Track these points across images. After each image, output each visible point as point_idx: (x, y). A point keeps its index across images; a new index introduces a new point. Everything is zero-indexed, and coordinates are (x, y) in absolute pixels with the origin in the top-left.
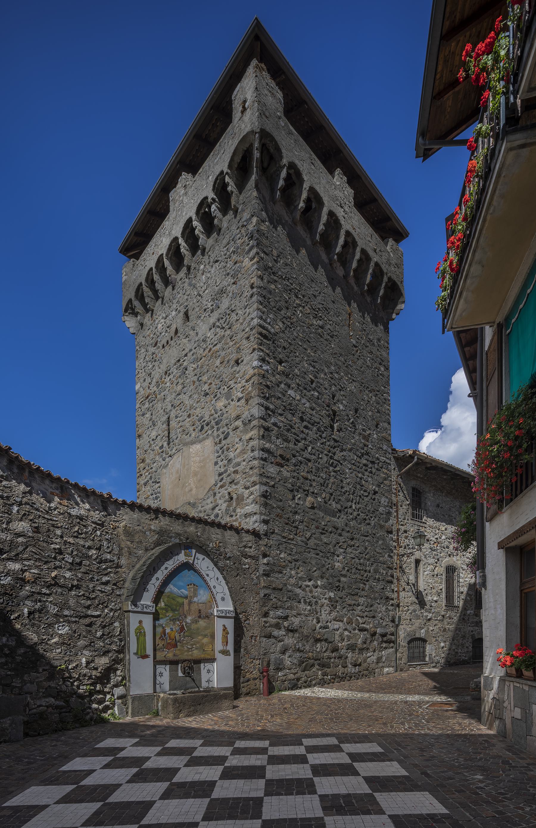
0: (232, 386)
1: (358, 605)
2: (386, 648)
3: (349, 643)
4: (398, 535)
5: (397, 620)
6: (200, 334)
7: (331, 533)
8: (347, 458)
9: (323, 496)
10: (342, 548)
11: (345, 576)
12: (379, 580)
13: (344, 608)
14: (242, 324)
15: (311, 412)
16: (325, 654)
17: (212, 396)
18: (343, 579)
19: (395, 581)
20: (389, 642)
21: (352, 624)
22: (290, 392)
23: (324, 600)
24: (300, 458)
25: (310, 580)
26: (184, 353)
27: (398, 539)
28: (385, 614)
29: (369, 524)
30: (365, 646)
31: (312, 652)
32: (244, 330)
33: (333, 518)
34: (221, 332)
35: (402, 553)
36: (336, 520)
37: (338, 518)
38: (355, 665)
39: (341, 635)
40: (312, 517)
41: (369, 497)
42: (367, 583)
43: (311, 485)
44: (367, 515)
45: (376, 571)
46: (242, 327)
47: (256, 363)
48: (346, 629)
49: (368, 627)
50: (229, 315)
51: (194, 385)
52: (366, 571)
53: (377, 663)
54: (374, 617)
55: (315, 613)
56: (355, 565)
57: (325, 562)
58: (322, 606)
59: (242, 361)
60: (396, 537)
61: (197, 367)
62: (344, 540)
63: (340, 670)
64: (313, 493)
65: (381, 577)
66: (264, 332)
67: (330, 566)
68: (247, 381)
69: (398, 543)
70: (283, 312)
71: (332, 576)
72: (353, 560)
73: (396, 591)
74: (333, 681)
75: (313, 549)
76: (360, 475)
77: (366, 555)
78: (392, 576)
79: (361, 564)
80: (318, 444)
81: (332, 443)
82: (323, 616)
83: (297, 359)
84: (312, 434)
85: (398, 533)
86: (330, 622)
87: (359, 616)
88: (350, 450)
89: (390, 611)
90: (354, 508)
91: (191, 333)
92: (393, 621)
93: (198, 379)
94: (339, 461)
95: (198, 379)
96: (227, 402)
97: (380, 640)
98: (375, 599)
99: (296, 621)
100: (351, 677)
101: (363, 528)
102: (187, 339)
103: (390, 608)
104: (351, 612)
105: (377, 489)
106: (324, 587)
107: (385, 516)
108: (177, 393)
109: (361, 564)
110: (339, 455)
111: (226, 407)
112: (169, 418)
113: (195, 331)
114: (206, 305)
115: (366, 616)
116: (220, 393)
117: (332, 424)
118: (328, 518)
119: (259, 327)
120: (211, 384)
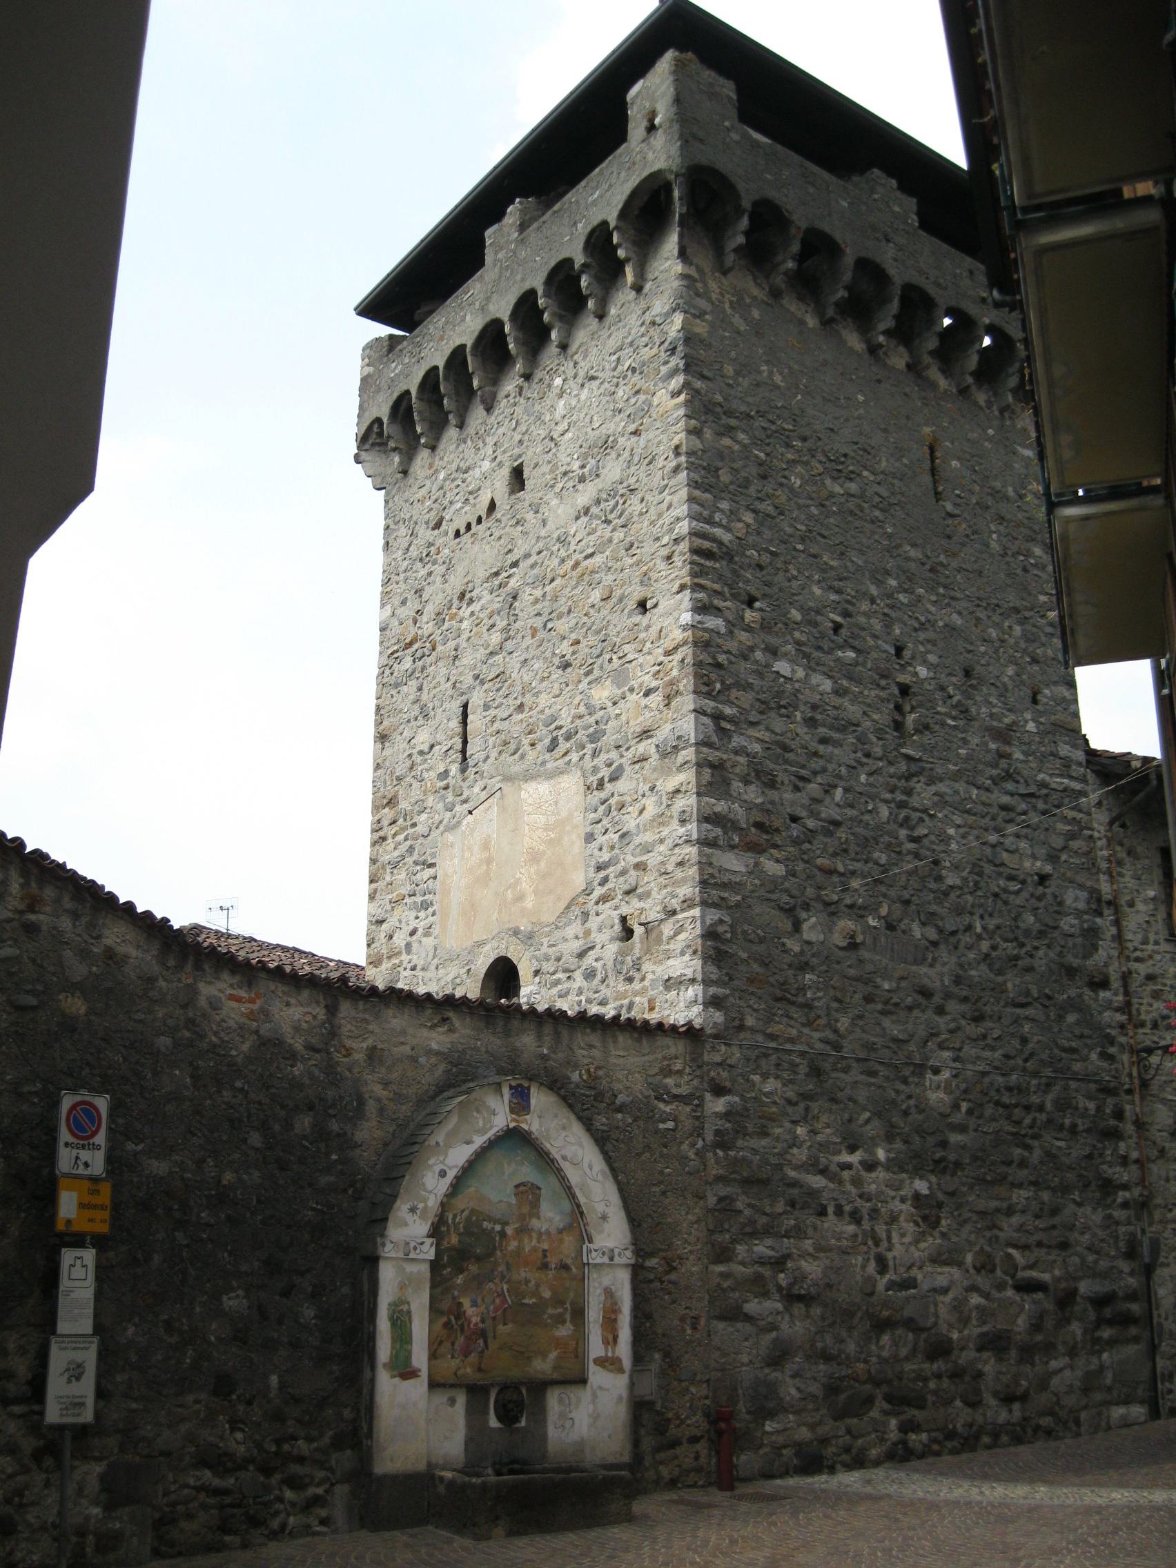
0: (630, 657)
1: (1010, 1212)
2: (1112, 1343)
3: (985, 1329)
4: (1126, 993)
6: (550, 525)
7: (910, 1009)
8: (947, 798)
9: (884, 911)
10: (948, 1049)
11: (962, 1129)
12: (1073, 1130)
13: (965, 1221)
14: (653, 523)
15: (837, 701)
16: (908, 1367)
17: (582, 672)
18: (955, 1138)
19: (1129, 1128)
20: (1126, 1320)
21: (993, 1271)
23: (897, 1202)
24: (811, 823)
26: (511, 558)
27: (1128, 1004)
28: (1101, 1234)
29: (1030, 969)
30: (1039, 1338)
31: (866, 1361)
32: (657, 539)
33: (914, 968)
34: (604, 531)
35: (1148, 1043)
36: (924, 970)
37: (931, 966)
39: (958, 1306)
41: (1025, 894)
42: (1036, 1143)
44: (1022, 945)
45: (1064, 1105)
46: (656, 531)
47: (687, 617)
48: (973, 1288)
49: (1046, 1277)
50: (622, 496)
51: (533, 637)
52: (1027, 1108)
53: (1086, 1390)
54: (1064, 1246)
55: (870, 1243)
56: (993, 1093)
57: (898, 1092)
58: (893, 1219)
59: (655, 606)
60: (1120, 998)
61: (544, 595)
62: (952, 1025)
63: (960, 1415)
64: (851, 907)
65: (1079, 1121)
66: (706, 544)
67: (912, 1102)
68: (668, 653)
69: (1130, 1014)
70: (752, 490)
71: (920, 1131)
72: (987, 1080)
73: (1137, 1161)
74: (936, 1447)
76: (993, 838)
77: (1026, 1060)
79: (1009, 1089)
80: (863, 778)
81: (903, 766)
82: (898, 1251)
83: (795, 584)
84: (843, 754)
85: (1125, 985)
86: (920, 1268)
87: (1015, 1246)
88: (956, 777)
89: (1117, 1223)
90: (979, 930)
91: (529, 515)
92: (1131, 1253)
93: (545, 625)
94: (925, 811)
95: (545, 625)
96: (619, 692)
97: (1092, 1316)
98: (1065, 1189)
100: (996, 1436)
101: (1012, 983)
102: (519, 528)
103: (1117, 1214)
104: (988, 1234)
105: (1048, 869)
106: (894, 1165)
107: (1079, 940)
108: (491, 649)
109: (1009, 1089)
110: (924, 794)
111: (615, 704)
113: (539, 515)
114: (568, 464)
115: (1040, 1244)
116: (601, 667)
117: (898, 718)
118: (901, 969)
119: (694, 539)
120: (577, 642)
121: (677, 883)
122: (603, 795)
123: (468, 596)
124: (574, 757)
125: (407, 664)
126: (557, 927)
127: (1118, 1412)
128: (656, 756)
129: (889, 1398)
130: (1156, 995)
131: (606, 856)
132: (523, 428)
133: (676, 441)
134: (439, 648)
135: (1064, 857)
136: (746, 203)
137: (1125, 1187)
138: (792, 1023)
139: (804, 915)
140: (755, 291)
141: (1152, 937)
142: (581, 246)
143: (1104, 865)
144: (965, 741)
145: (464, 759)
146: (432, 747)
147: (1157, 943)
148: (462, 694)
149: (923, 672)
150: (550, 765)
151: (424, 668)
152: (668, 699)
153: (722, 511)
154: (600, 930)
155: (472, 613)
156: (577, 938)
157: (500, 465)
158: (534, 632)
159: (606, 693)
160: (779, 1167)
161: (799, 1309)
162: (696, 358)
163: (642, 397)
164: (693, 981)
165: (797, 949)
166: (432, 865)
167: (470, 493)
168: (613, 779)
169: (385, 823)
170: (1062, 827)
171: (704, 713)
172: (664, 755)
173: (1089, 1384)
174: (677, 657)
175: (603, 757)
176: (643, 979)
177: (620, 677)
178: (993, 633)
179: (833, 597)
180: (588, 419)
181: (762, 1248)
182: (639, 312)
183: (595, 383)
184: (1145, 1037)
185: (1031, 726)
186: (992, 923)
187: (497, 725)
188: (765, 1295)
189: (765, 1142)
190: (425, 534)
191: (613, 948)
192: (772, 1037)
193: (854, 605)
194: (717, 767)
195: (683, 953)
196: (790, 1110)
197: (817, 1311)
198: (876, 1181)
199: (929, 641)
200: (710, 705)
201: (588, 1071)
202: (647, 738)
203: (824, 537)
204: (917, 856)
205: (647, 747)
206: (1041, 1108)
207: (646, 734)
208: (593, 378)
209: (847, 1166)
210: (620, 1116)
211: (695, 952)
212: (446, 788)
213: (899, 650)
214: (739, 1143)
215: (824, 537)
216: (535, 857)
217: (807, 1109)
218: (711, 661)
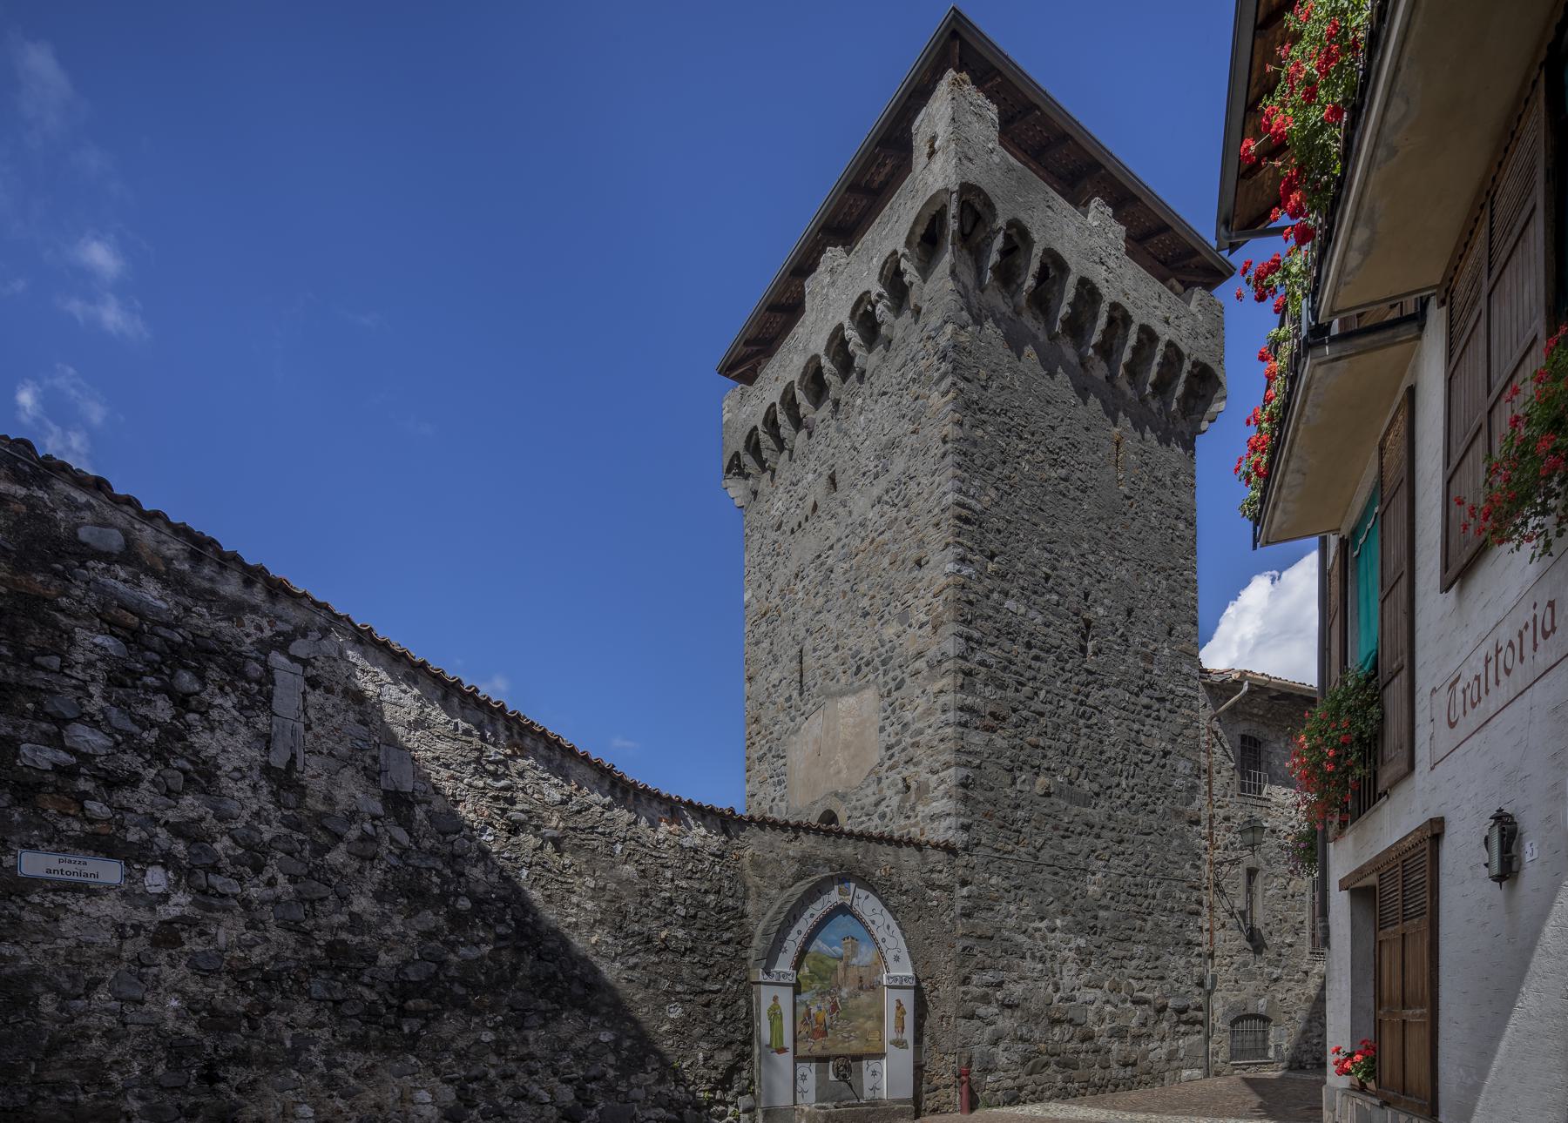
1: (1132, 958)
2: (1185, 1034)
4: (1211, 827)
5: (1208, 982)
6: (855, 513)
9: (1067, 772)
11: (1107, 908)
12: (1172, 911)
14: (926, 500)
15: (1046, 630)
16: (1069, 1046)
18: (1102, 913)
19: (1205, 911)
22: (1010, 604)
24: (1025, 713)
25: (1042, 919)
27: (1211, 834)
28: (1184, 972)
29: (1153, 812)
30: (1144, 1030)
34: (891, 513)
36: (1089, 810)
38: (1125, 1065)
39: (1099, 1012)
40: (1046, 811)
43: (1045, 757)
45: (1167, 896)
46: (927, 506)
48: (1108, 1002)
49: (1150, 996)
53: (1169, 1061)
54: (1162, 978)
63: (1097, 1074)
64: (1048, 769)
66: (965, 512)
71: (1083, 910)
76: (1136, 726)
78: (1200, 903)
81: (1083, 677)
82: (1066, 979)
83: (1021, 545)
84: (1047, 668)
88: (1117, 685)
91: (840, 510)
92: (1201, 984)
97: (1175, 1018)
98: (1165, 945)
99: (1018, 990)
100: (1117, 1086)
101: (1142, 819)
103: (1194, 960)
105: (1169, 747)
106: (1067, 930)
110: (1096, 697)
118: (1075, 809)
121: (940, 753)
124: (871, 677)
127: (1186, 1073)
129: (1058, 1064)
130: (1229, 830)
131: (893, 741)
132: (835, 443)
137: (1200, 945)
143: (1204, 746)
144: (1124, 661)
150: (856, 684)
152: (935, 628)
157: (820, 475)
158: (845, 593)
159: (892, 631)
160: (999, 930)
161: (1008, 1012)
168: (898, 688)
170: (1181, 721)
172: (931, 667)
173: (1171, 1056)
174: (943, 597)
175: (891, 674)
177: (903, 618)
178: (1149, 586)
181: (988, 977)
185: (1167, 651)
186: (1132, 782)
190: (772, 535)
192: (997, 850)
194: (968, 673)
197: (1018, 1013)
198: (1055, 939)
204: (1089, 737)
205: (921, 664)
206: (1154, 897)
207: (920, 655)
209: (1037, 930)
216: (847, 746)
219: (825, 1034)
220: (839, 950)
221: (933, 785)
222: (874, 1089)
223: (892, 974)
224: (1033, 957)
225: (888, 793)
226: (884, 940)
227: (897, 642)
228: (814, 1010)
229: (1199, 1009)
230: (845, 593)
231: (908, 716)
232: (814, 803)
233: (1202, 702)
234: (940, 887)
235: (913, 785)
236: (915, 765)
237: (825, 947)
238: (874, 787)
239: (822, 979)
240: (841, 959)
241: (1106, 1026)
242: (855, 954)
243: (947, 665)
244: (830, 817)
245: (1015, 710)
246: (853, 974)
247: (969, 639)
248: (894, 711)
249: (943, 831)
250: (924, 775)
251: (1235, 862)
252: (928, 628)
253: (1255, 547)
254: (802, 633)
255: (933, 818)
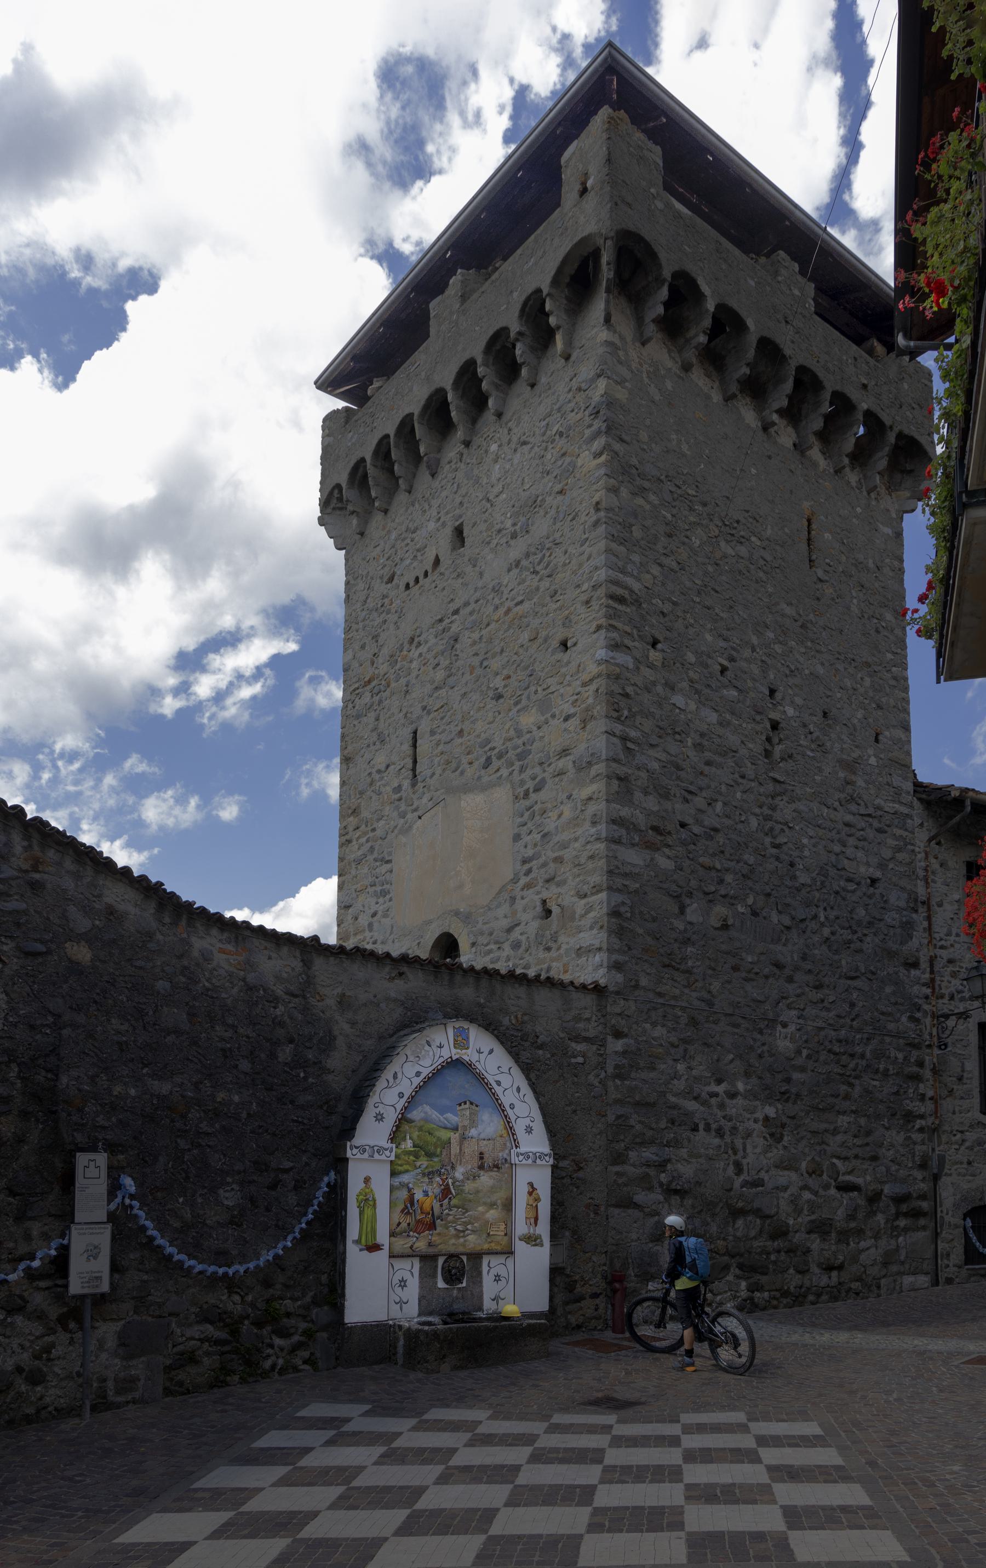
0: (552, 689)
1: (835, 1132)
2: (906, 1230)
3: (813, 1217)
4: (932, 972)
5: (935, 1163)
7: (767, 977)
8: (803, 815)
9: (750, 901)
10: (795, 1009)
11: (803, 1069)
12: (886, 1074)
13: (802, 1138)
16: (756, 1244)
17: (512, 702)
18: (796, 1076)
19: (927, 1074)
20: (916, 1214)
21: (821, 1175)
23: (751, 1122)
24: (696, 829)
25: (719, 1082)
26: (453, 606)
27: (933, 980)
30: (853, 1225)
31: (724, 1239)
32: (578, 586)
33: (771, 946)
37: (784, 945)
38: (829, 1268)
39: (794, 1201)
40: (724, 947)
41: (859, 893)
42: (857, 1082)
43: (721, 881)
44: (855, 932)
47: (601, 653)
48: (805, 1187)
49: (860, 1181)
50: (548, 549)
51: (471, 674)
52: (852, 1056)
53: (885, 1264)
54: (874, 1158)
55: (730, 1152)
56: (827, 1043)
57: (754, 1040)
58: (749, 1135)
59: (575, 644)
60: (927, 976)
61: (481, 638)
62: (799, 991)
63: (793, 1280)
64: (724, 896)
65: (891, 1067)
66: (620, 591)
67: (765, 1048)
68: (584, 684)
69: (934, 989)
72: (822, 1033)
73: (931, 1099)
74: (775, 1302)
75: (726, 1015)
76: (837, 848)
77: (853, 1020)
78: (921, 1064)
79: (840, 1041)
80: (739, 795)
81: (770, 787)
82: (751, 1159)
83: (691, 631)
85: (932, 966)
86: (767, 1172)
87: (839, 1158)
89: (915, 1143)
90: (822, 919)
91: (469, 569)
92: (923, 1166)
93: (481, 664)
94: (786, 824)
95: (481, 664)
96: (543, 718)
99: (687, 1171)
100: (819, 1295)
102: (460, 581)
103: (917, 1137)
104: (818, 1148)
105: (878, 874)
107: (899, 931)
108: (436, 684)
109: (840, 1041)
110: (786, 811)
111: (539, 728)
112: (415, 733)
113: (477, 569)
114: (502, 523)
115: (856, 1157)
116: (528, 698)
117: (769, 747)
119: (610, 585)
120: (509, 677)
122: (527, 803)
123: (416, 640)
125: (367, 698)
126: (490, 909)
127: (908, 1280)
128: (573, 771)
129: (741, 1267)
132: (463, 491)
133: (596, 498)
134: (393, 685)
135: (891, 866)
136: (667, 273)
137: (922, 1117)
138: (676, 985)
139: (688, 901)
140: (670, 364)
141: (954, 931)
142: (517, 314)
144: (820, 770)
145: (415, 776)
146: (388, 766)
147: (958, 935)
148: (412, 723)
149: (790, 711)
151: (380, 702)
153: (634, 563)
154: (524, 910)
155: (420, 655)
156: (506, 917)
157: (444, 525)
158: (472, 669)
159: (532, 720)
160: (663, 1094)
161: (675, 1199)
162: (614, 423)
163: (568, 459)
164: (600, 949)
165: (682, 927)
166: (389, 862)
167: (418, 550)
169: (350, 829)
171: (614, 735)
174: (593, 687)
176: (559, 948)
177: (544, 706)
179: (722, 644)
180: (519, 482)
181: (649, 1154)
182: (567, 379)
183: (526, 448)
184: (944, 1006)
186: (832, 914)
187: (441, 747)
188: (650, 1189)
189: (652, 1075)
191: (535, 925)
193: (738, 652)
195: (591, 928)
196: (673, 1051)
197: (689, 1202)
198: (735, 1107)
199: (796, 686)
200: (618, 728)
201: (516, 1017)
202: (566, 755)
203: (717, 592)
204: (777, 859)
206: (863, 1056)
208: (525, 443)
210: (541, 1052)
211: (602, 927)
212: (400, 799)
213: (772, 692)
214: (633, 1075)
215: (717, 592)
217: (686, 1050)
218: (621, 691)
219: (432, 1226)
220: (453, 1119)
221: (579, 911)
222: (496, 1299)
223: (523, 1149)
224: (708, 1128)
225: (524, 917)
226: (512, 1106)
227: (537, 734)
228: (419, 1195)
229: (923, 1197)
230: (472, 669)
231: (550, 826)
232: (429, 922)
233: (918, 821)
234: (586, 1040)
235: (555, 910)
236: (558, 885)
237: (435, 1115)
238: (505, 909)
239: (430, 1155)
240: (456, 1129)
241: (805, 1219)
242: (473, 1123)
243: (594, 770)
244: (448, 944)
245: (683, 825)
246: (471, 1149)
247: (624, 739)
248: (533, 816)
249: (591, 971)
250: (569, 899)
251: (964, 1015)
252: (574, 723)
253: (938, 682)
254: (417, 711)
255: (580, 952)
